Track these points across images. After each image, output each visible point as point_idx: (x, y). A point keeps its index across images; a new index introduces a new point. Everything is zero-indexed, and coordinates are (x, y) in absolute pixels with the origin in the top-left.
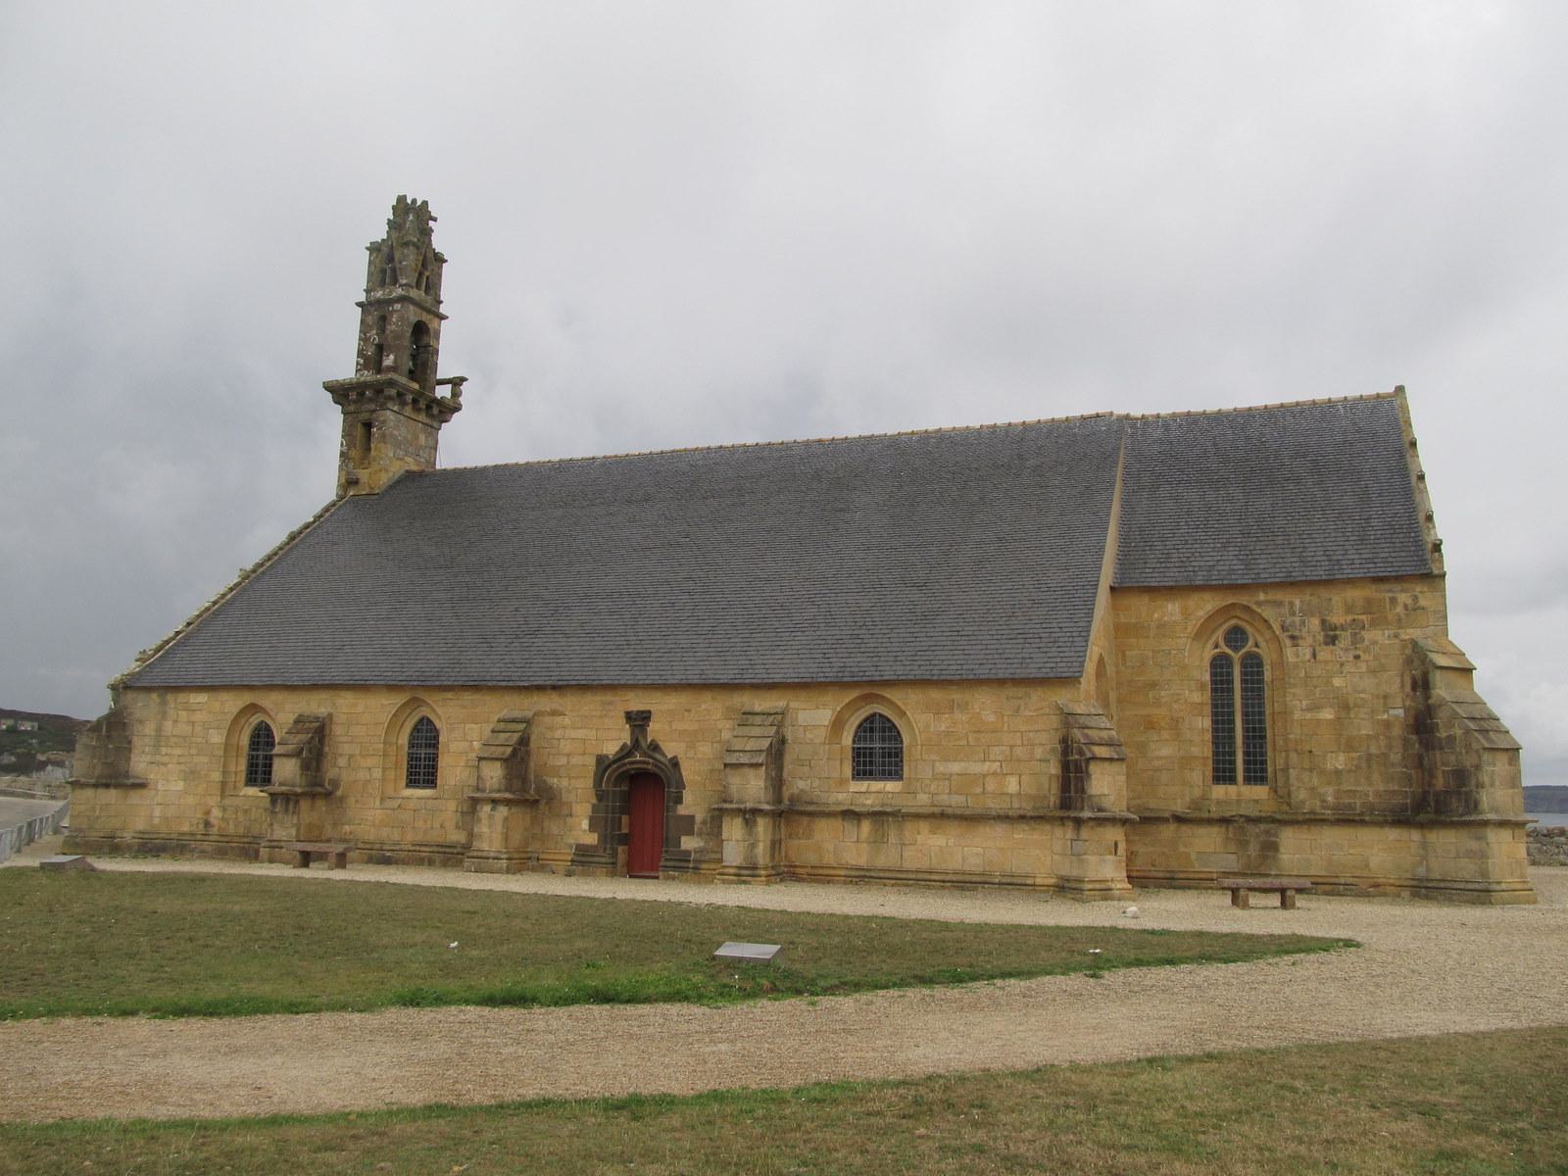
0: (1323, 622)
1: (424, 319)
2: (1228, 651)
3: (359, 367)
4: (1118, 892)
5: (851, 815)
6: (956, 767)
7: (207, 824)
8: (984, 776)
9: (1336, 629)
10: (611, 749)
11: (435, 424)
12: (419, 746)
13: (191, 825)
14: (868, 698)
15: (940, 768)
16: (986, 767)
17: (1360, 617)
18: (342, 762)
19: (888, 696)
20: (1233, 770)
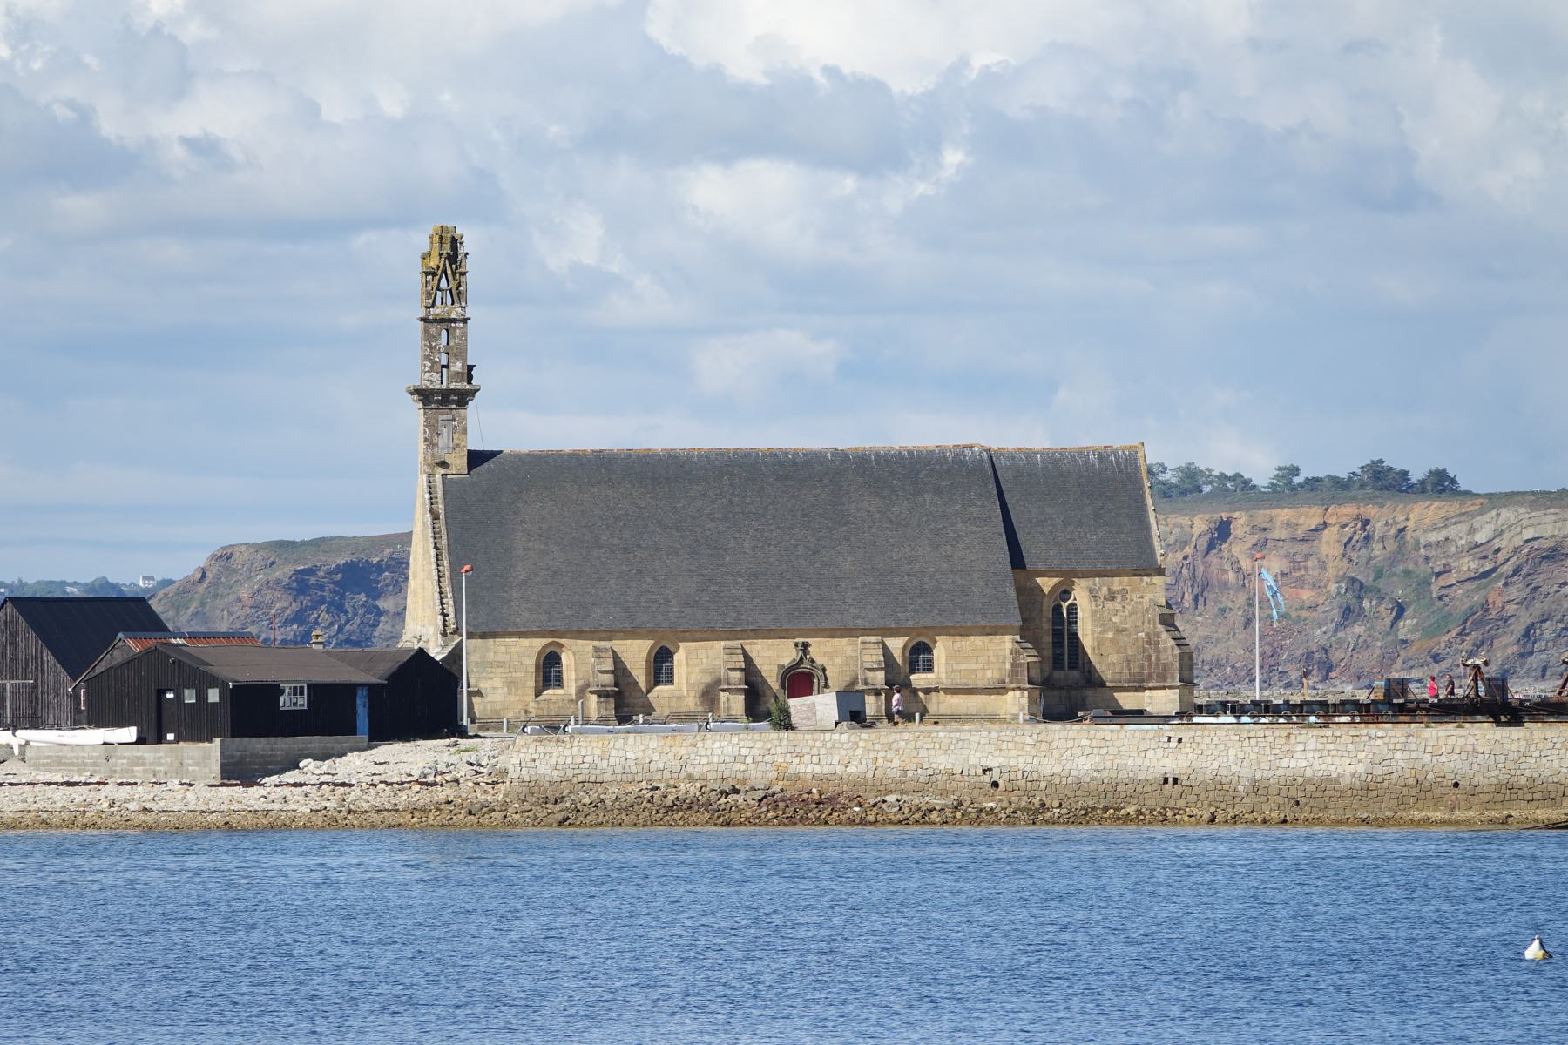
0: (1109, 589)
3: (427, 369)
6: (963, 666)
7: (526, 712)
8: (975, 670)
14: (919, 635)
15: (955, 667)
16: (977, 666)
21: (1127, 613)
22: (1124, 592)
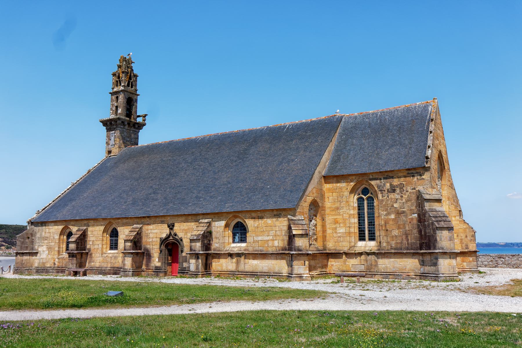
1: (131, 97)
2: (363, 196)
3: (111, 114)
4: (305, 278)
5: (231, 255)
7: (54, 264)
8: (268, 241)
9: (395, 187)
10: (164, 236)
11: (137, 130)
12: (113, 237)
13: (50, 265)
14: (236, 217)
15: (255, 239)
17: (403, 183)
18: (91, 243)
19: (240, 216)
20: (364, 236)
21: (404, 201)
22: (401, 186)
